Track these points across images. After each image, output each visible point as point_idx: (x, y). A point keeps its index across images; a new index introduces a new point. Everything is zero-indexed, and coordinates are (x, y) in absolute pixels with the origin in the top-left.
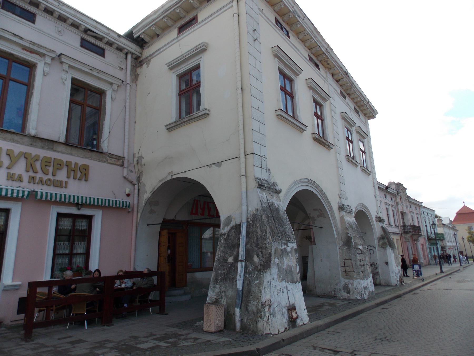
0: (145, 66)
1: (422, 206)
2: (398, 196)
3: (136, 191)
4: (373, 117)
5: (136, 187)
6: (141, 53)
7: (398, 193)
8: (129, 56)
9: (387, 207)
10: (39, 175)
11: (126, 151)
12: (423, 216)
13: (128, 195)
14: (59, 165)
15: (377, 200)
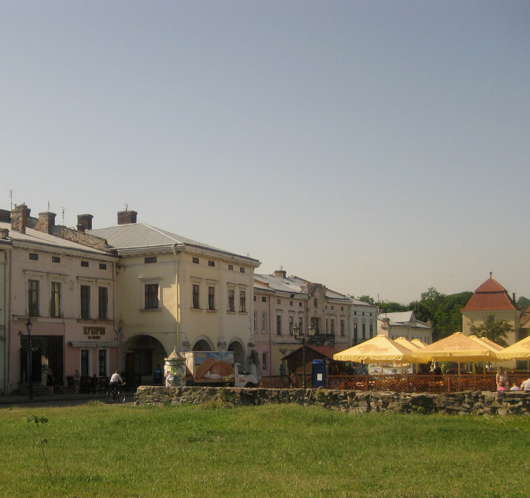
0: (122, 269)
1: (352, 305)
2: (309, 301)
3: (119, 336)
4: (257, 267)
5: (119, 334)
6: (120, 261)
7: (309, 298)
8: (114, 265)
9: (292, 315)
10: (94, 335)
11: (115, 317)
12: (352, 317)
13: (116, 339)
14: (97, 329)
15: (251, 331)
